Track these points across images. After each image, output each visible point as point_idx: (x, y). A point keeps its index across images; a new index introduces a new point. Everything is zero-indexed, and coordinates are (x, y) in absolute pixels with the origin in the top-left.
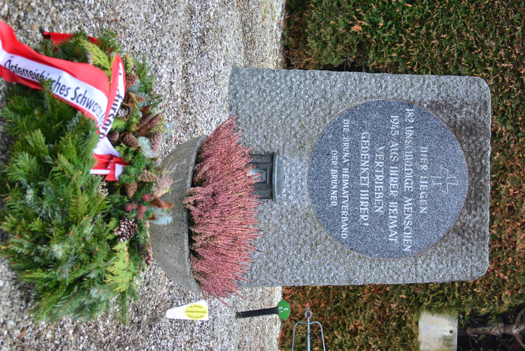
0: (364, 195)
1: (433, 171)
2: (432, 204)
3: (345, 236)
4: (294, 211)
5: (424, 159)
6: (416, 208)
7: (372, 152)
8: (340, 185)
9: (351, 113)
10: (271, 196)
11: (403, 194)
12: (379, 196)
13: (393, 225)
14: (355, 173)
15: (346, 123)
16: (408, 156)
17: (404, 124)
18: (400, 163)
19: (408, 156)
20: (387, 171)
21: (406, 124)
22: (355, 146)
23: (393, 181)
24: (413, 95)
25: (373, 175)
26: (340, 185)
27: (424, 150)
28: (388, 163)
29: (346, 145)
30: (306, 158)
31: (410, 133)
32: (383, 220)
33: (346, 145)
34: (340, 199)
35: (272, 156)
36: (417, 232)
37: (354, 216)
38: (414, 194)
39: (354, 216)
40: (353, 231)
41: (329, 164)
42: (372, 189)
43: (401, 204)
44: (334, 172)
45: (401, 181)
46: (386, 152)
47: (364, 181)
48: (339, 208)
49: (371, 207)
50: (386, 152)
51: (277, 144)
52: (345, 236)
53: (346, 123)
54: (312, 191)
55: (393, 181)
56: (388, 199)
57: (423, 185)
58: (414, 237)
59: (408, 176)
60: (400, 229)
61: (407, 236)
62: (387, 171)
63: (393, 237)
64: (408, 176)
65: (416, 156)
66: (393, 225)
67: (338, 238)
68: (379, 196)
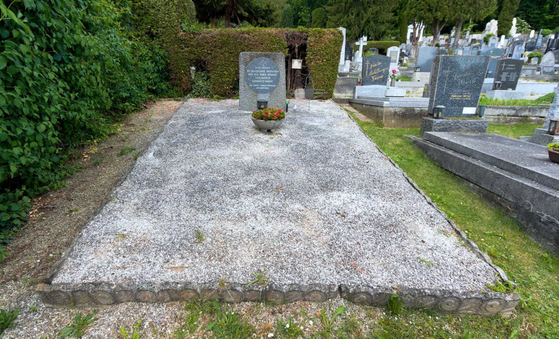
0: (266, 81)
1: (261, 66)
2: (268, 66)
3: (275, 86)
4: (270, 97)
5: (258, 68)
6: (269, 70)
7: (257, 79)
8: (264, 87)
9: (248, 84)
10: (267, 102)
11: (266, 73)
12: (266, 78)
13: (273, 75)
14: (261, 83)
15: (251, 85)
16: (258, 71)
17: (250, 72)
18: (259, 73)
19: (258, 71)
20: (261, 76)
21: (250, 72)
22: (255, 83)
23: (263, 75)
24: (243, 70)
25: (262, 79)
26: (264, 87)
27: (256, 67)
28: (259, 76)
29: (255, 85)
30: (258, 94)
31: (252, 71)
32: (271, 77)
33: (255, 85)
34: (267, 87)
35: (258, 102)
36: (274, 69)
37: (271, 84)
38: (266, 70)
39: (271, 84)
40: (274, 84)
41: (260, 89)
42: (265, 80)
43: (268, 73)
44: (261, 88)
45: (263, 73)
46: (257, 76)
47: (263, 81)
48: (269, 87)
49: (269, 80)
50: (257, 76)
51: (255, 101)
52: (275, 86)
53: (251, 85)
54: (265, 93)
55: (263, 75)
56: (267, 76)
57: (264, 68)
58: (275, 70)
59: (262, 71)
60: (274, 73)
61: (275, 72)
62: (261, 76)
63: (275, 75)
64: (262, 71)
65: (257, 69)
66: (273, 75)
67: (276, 87)
68: (266, 78)
